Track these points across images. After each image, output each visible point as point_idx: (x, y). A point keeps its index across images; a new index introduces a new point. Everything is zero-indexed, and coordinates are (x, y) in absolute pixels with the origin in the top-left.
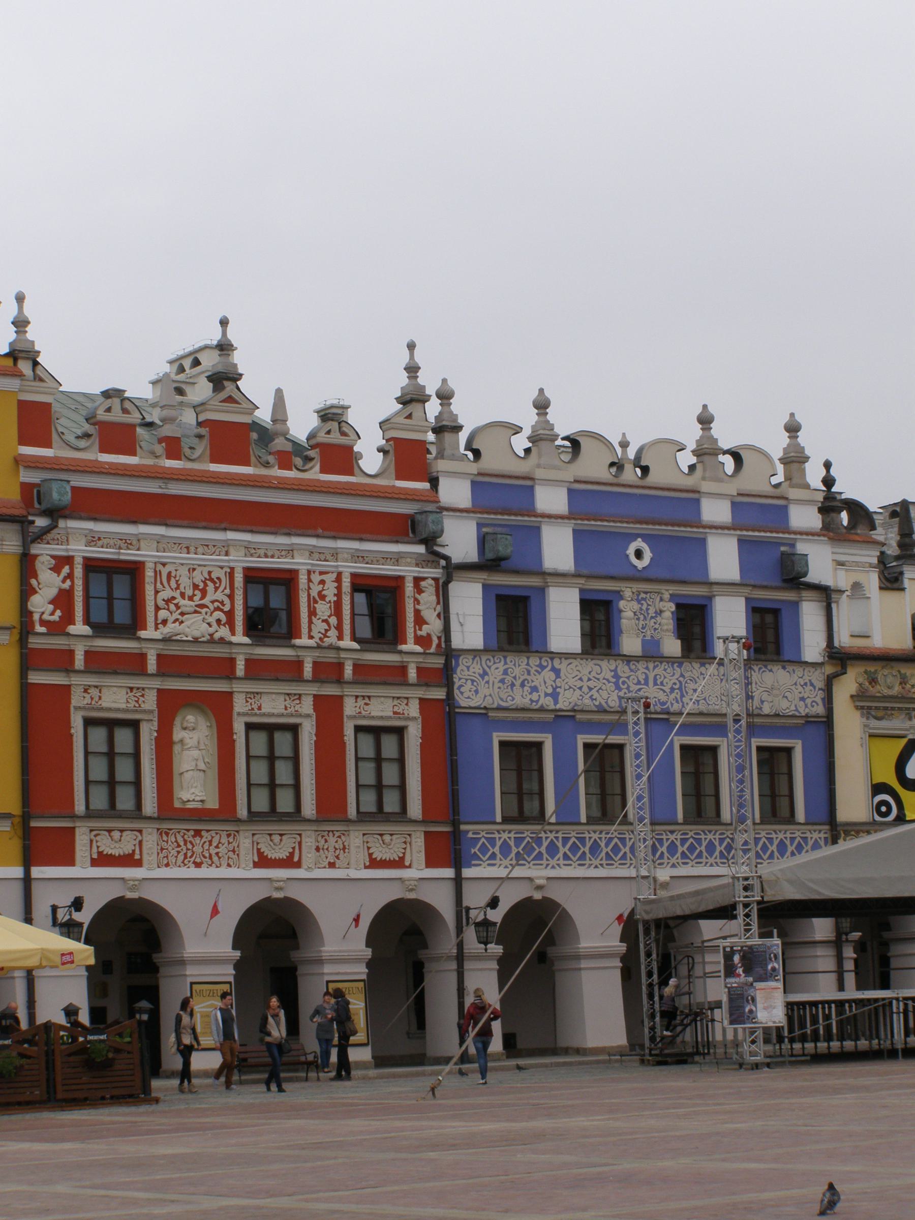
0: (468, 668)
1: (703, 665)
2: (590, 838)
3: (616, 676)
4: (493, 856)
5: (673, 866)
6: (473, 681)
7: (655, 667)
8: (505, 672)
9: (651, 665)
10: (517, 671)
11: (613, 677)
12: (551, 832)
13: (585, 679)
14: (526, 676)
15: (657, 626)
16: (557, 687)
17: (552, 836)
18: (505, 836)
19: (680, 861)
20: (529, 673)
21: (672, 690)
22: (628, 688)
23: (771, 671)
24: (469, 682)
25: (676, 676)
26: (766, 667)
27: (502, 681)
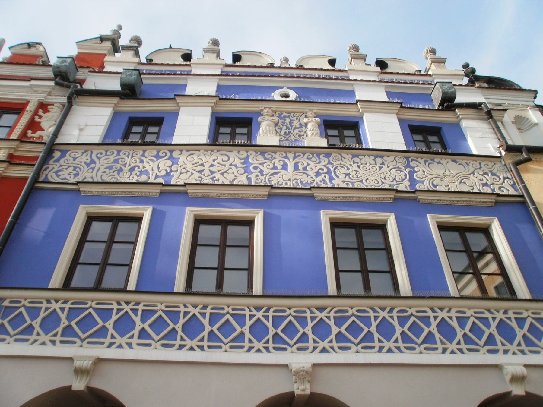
0: (75, 159)
1: (354, 156)
2: (186, 313)
3: (246, 162)
4: (29, 329)
5: (324, 350)
6: (75, 168)
7: (295, 158)
8: (116, 161)
9: (291, 156)
10: (128, 160)
11: (243, 163)
12: (128, 303)
13: (207, 166)
14: (138, 164)
15: (302, 133)
16: (171, 171)
17: (127, 308)
18: (55, 306)
19: (335, 345)
20: (142, 161)
21: (318, 174)
22: (261, 172)
23: (439, 163)
24: (72, 168)
25: (323, 163)
26: (433, 160)
27: (110, 168)
